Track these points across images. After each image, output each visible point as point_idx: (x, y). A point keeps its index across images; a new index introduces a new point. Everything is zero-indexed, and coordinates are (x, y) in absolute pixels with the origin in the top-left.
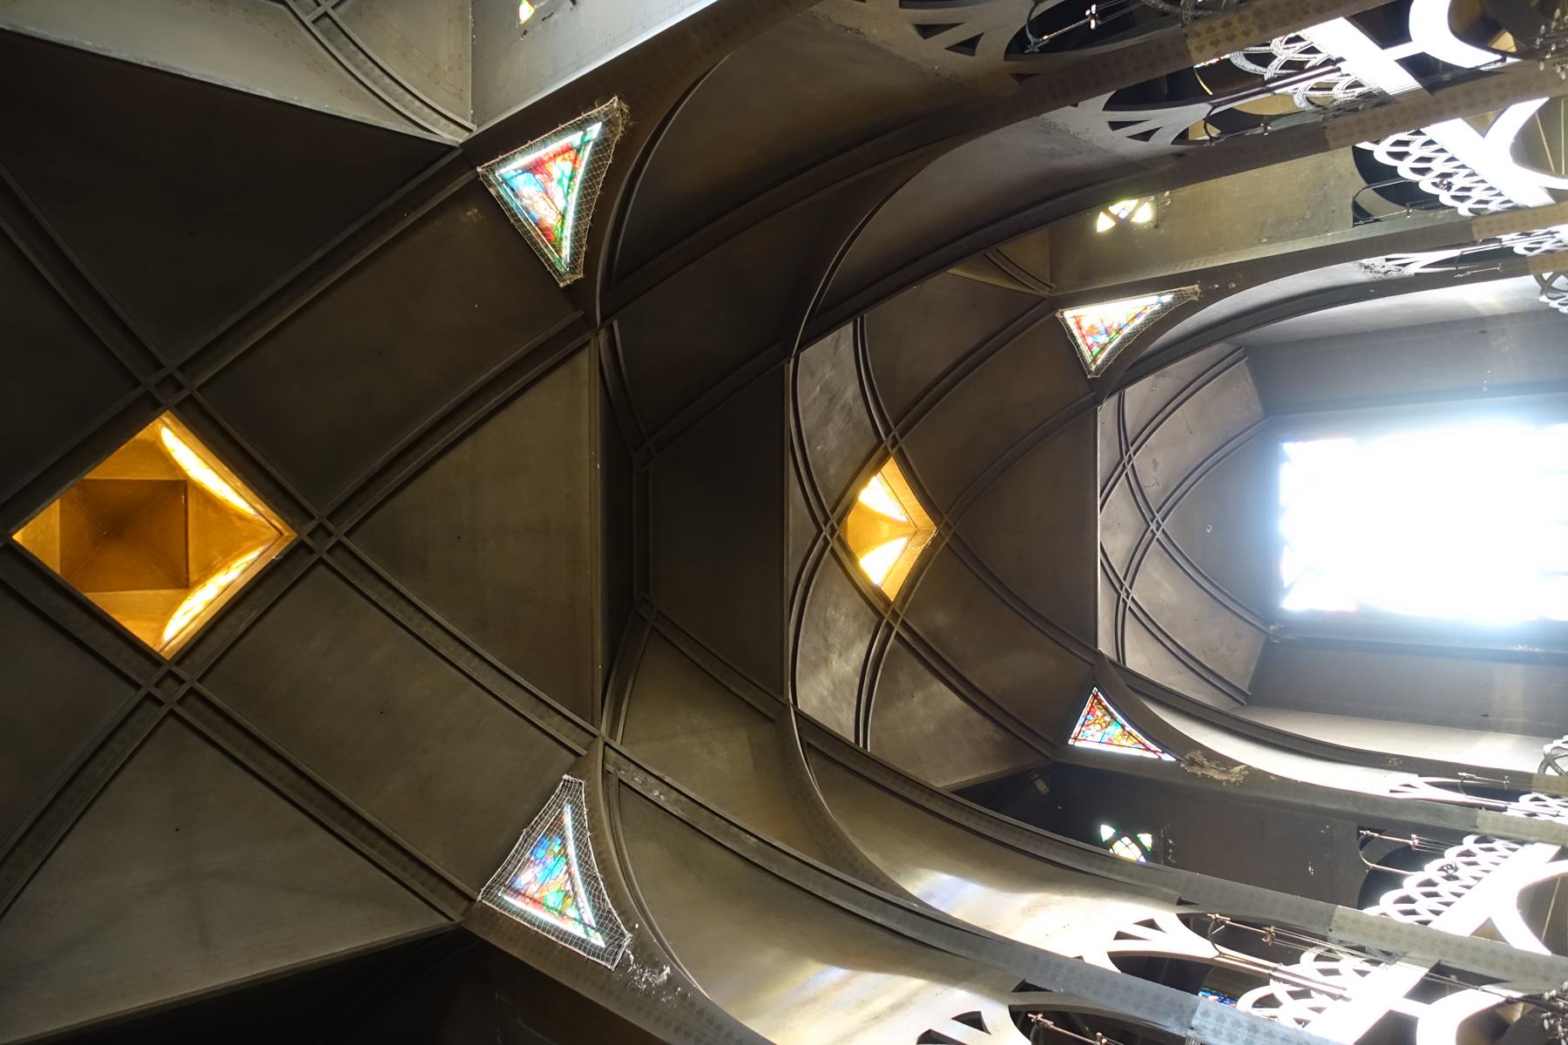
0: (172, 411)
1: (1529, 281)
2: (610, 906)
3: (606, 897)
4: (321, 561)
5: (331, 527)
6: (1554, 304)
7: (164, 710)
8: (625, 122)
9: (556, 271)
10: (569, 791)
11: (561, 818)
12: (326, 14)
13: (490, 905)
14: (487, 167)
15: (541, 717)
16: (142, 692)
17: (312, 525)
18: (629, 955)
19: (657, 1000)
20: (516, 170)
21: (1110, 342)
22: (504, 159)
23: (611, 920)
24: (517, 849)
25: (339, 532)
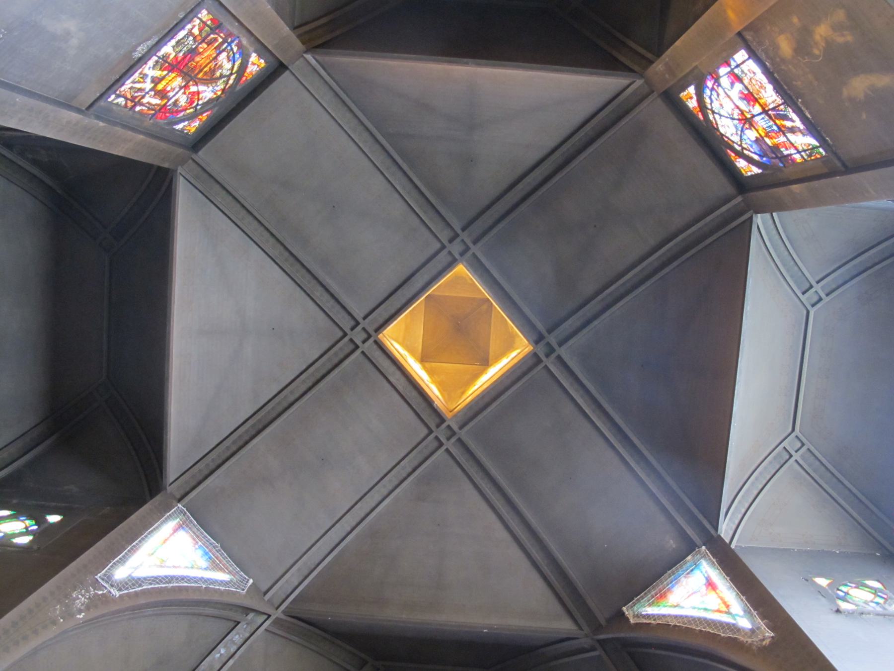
0: (533, 350)
2: (145, 587)
3: (152, 586)
4: (431, 432)
5: (453, 440)
7: (348, 330)
8: (755, 643)
9: (635, 604)
10: (240, 581)
11: (221, 570)
12: (791, 456)
13: (173, 511)
14: (707, 553)
15: (299, 570)
16: (360, 320)
17: (455, 427)
18: (103, 591)
19: (59, 602)
20: (706, 572)
22: (714, 563)
23: (134, 585)
24: (207, 537)
25: (450, 445)
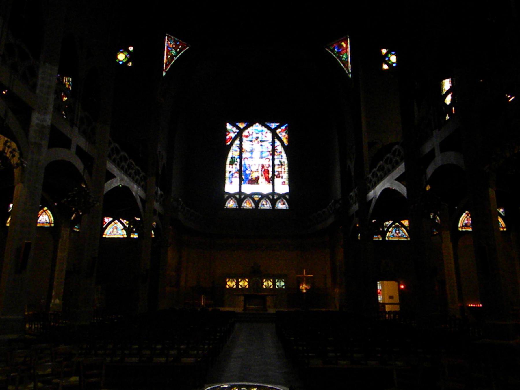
1: (339, 196)
6: (330, 204)
21: (334, 54)
